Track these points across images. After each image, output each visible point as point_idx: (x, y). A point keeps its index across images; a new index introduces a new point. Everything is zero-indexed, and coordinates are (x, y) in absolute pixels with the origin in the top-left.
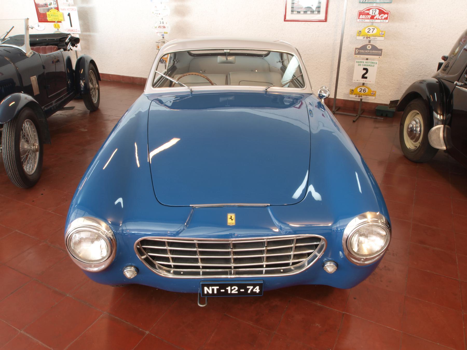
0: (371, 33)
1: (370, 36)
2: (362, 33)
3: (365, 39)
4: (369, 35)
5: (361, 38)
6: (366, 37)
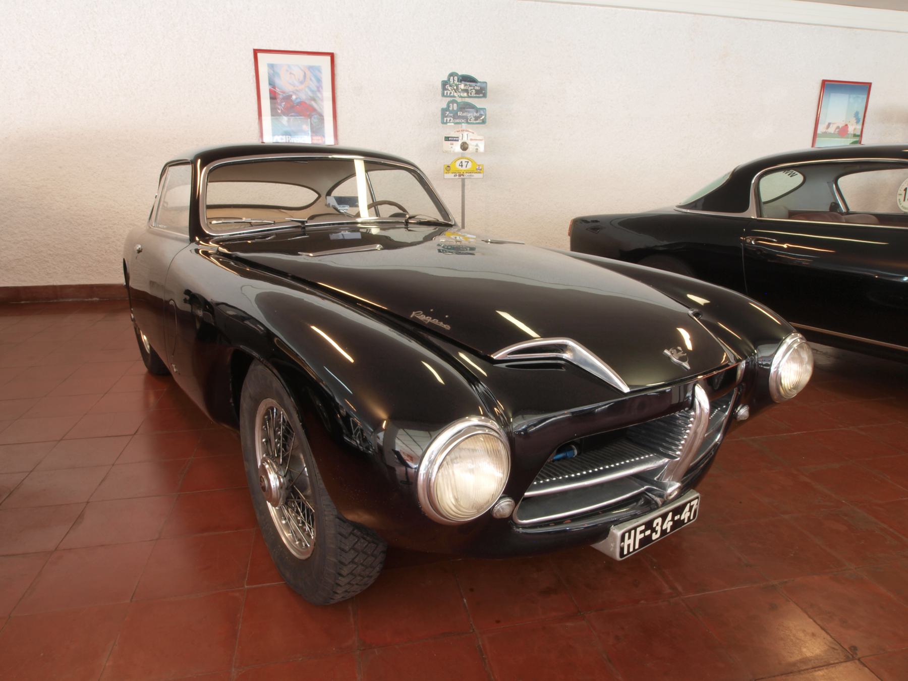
0: (464, 167)
1: (463, 173)
2: (452, 169)
5: (450, 176)
6: (458, 174)
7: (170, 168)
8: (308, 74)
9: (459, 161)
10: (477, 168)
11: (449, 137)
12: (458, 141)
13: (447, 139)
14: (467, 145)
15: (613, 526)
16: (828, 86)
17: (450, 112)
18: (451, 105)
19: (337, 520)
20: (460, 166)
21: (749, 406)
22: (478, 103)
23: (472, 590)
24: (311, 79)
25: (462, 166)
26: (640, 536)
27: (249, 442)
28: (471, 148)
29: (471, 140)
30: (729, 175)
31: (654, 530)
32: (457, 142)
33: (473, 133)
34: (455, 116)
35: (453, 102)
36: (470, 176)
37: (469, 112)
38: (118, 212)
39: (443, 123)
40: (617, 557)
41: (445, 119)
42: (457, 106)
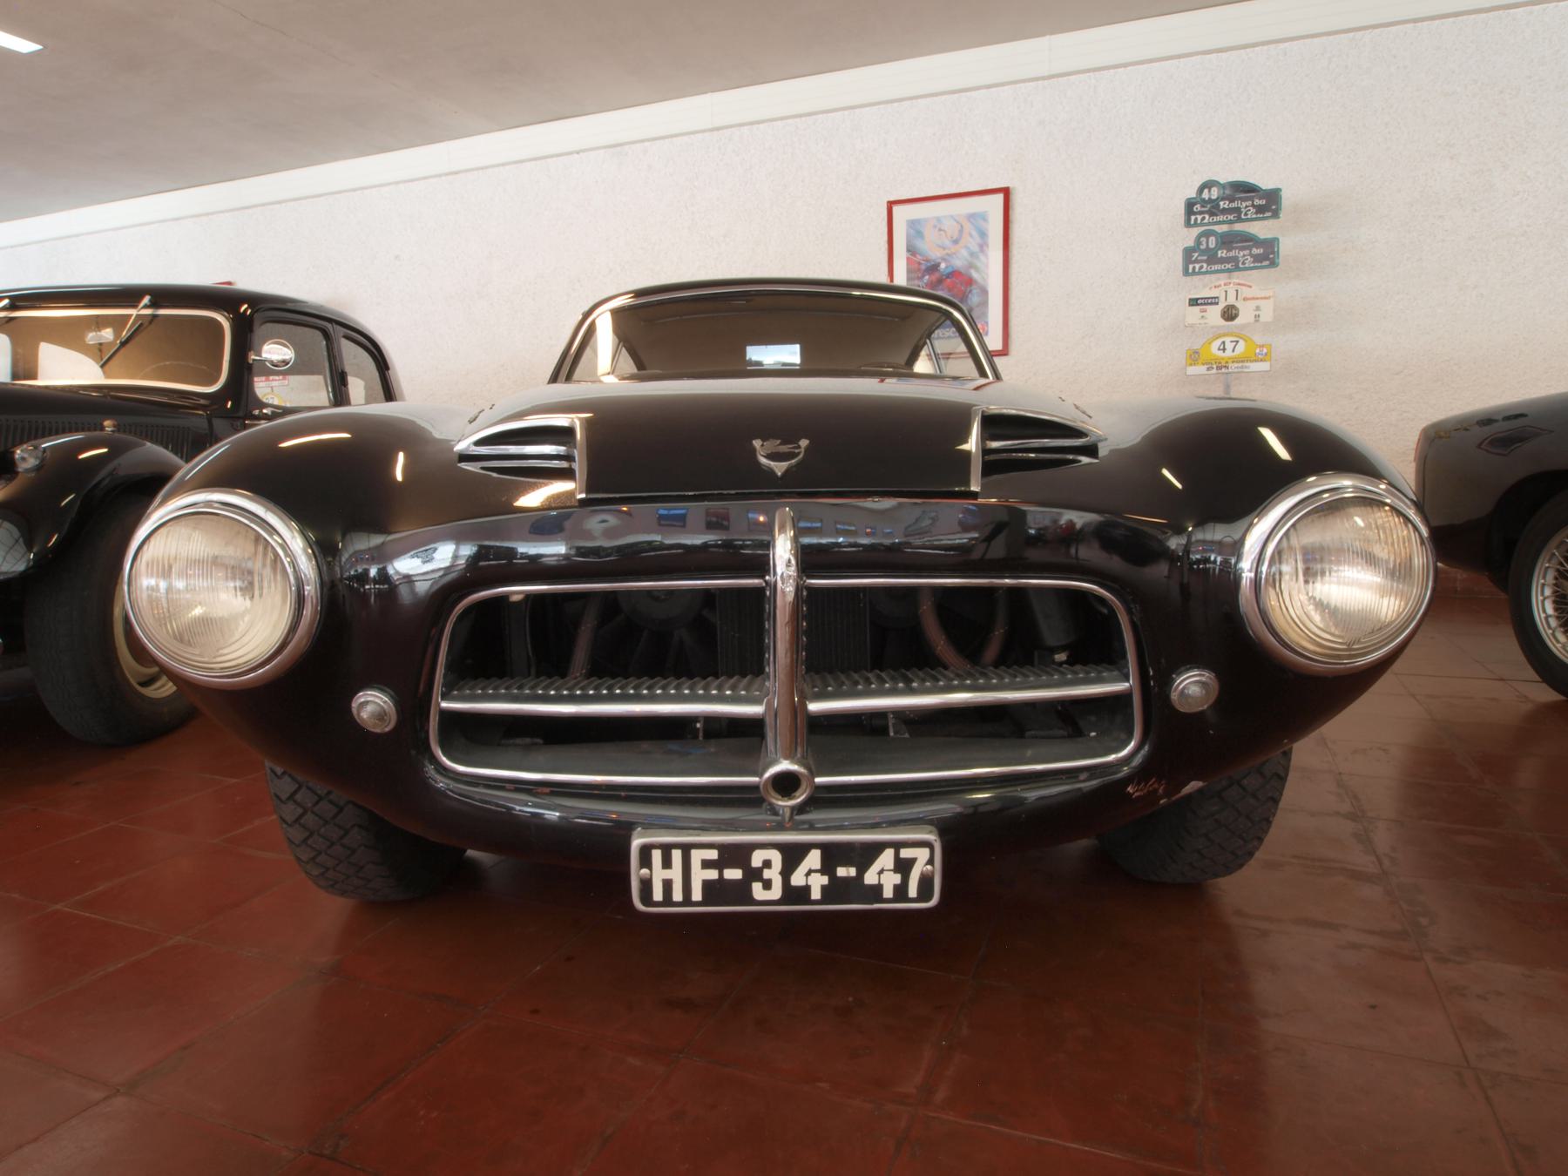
0: (1229, 353)
1: (1227, 362)
3: (1214, 371)
4: (1223, 359)
5: (1200, 369)
6: (1215, 366)
8: (968, 227)
9: (1218, 342)
10: (1258, 351)
11: (1197, 299)
12: (1217, 304)
13: (1194, 302)
14: (1237, 309)
15: (639, 829)
17: (1203, 252)
18: (1203, 240)
20: (1219, 349)
21: (1220, 676)
22: (1261, 229)
24: (971, 235)
25: (1224, 350)
26: (700, 876)
28: (1245, 317)
29: (1245, 299)
31: (754, 875)
33: (1250, 287)
34: (1212, 259)
35: (1207, 234)
36: (1242, 367)
39: (1186, 273)
41: (1191, 267)
42: (1217, 240)
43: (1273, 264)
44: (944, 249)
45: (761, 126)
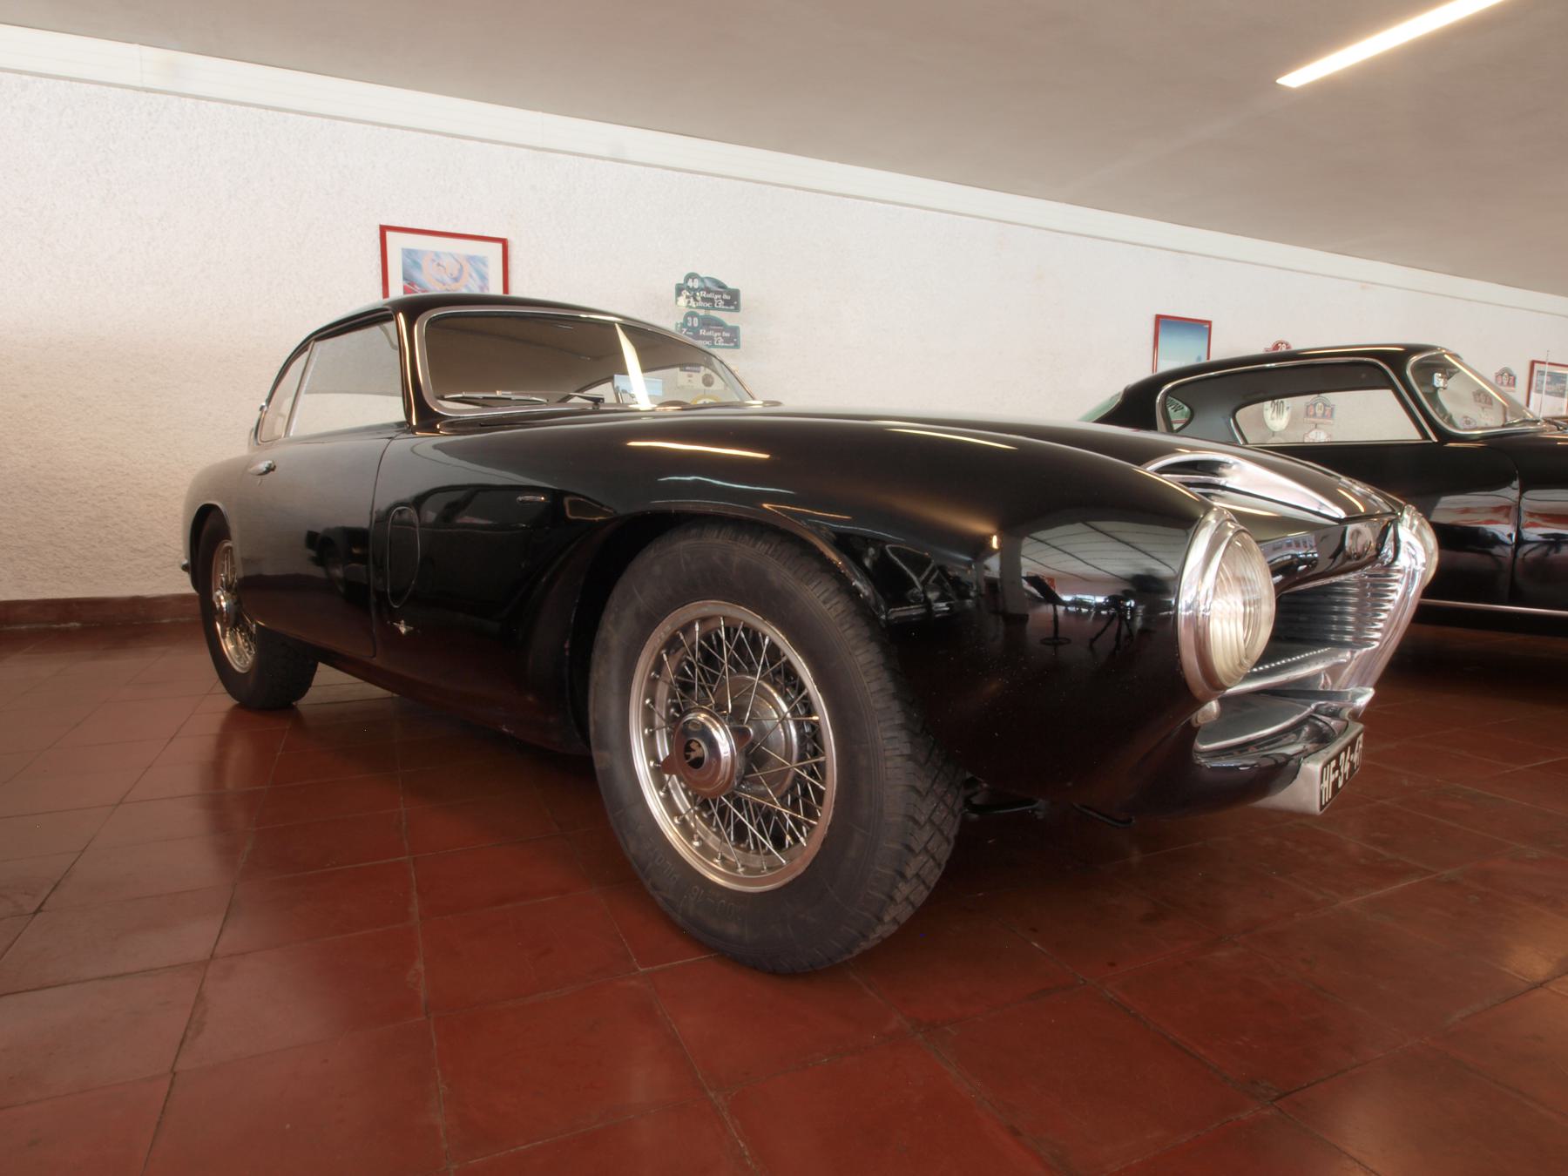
7: (316, 344)
8: (468, 268)
16: (1161, 321)
18: (689, 319)
19: (911, 764)
23: (1034, 930)
24: (471, 276)
27: (614, 712)
30: (1121, 395)
32: (697, 374)
37: (716, 331)
38: (128, 474)
40: (1316, 808)
43: (737, 346)
44: (444, 284)
45: (212, 105)
